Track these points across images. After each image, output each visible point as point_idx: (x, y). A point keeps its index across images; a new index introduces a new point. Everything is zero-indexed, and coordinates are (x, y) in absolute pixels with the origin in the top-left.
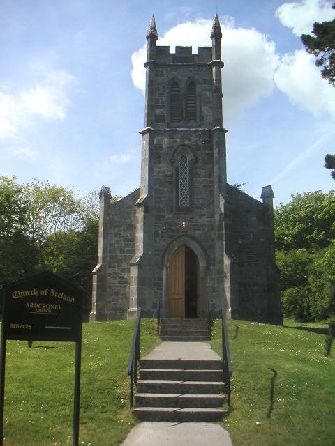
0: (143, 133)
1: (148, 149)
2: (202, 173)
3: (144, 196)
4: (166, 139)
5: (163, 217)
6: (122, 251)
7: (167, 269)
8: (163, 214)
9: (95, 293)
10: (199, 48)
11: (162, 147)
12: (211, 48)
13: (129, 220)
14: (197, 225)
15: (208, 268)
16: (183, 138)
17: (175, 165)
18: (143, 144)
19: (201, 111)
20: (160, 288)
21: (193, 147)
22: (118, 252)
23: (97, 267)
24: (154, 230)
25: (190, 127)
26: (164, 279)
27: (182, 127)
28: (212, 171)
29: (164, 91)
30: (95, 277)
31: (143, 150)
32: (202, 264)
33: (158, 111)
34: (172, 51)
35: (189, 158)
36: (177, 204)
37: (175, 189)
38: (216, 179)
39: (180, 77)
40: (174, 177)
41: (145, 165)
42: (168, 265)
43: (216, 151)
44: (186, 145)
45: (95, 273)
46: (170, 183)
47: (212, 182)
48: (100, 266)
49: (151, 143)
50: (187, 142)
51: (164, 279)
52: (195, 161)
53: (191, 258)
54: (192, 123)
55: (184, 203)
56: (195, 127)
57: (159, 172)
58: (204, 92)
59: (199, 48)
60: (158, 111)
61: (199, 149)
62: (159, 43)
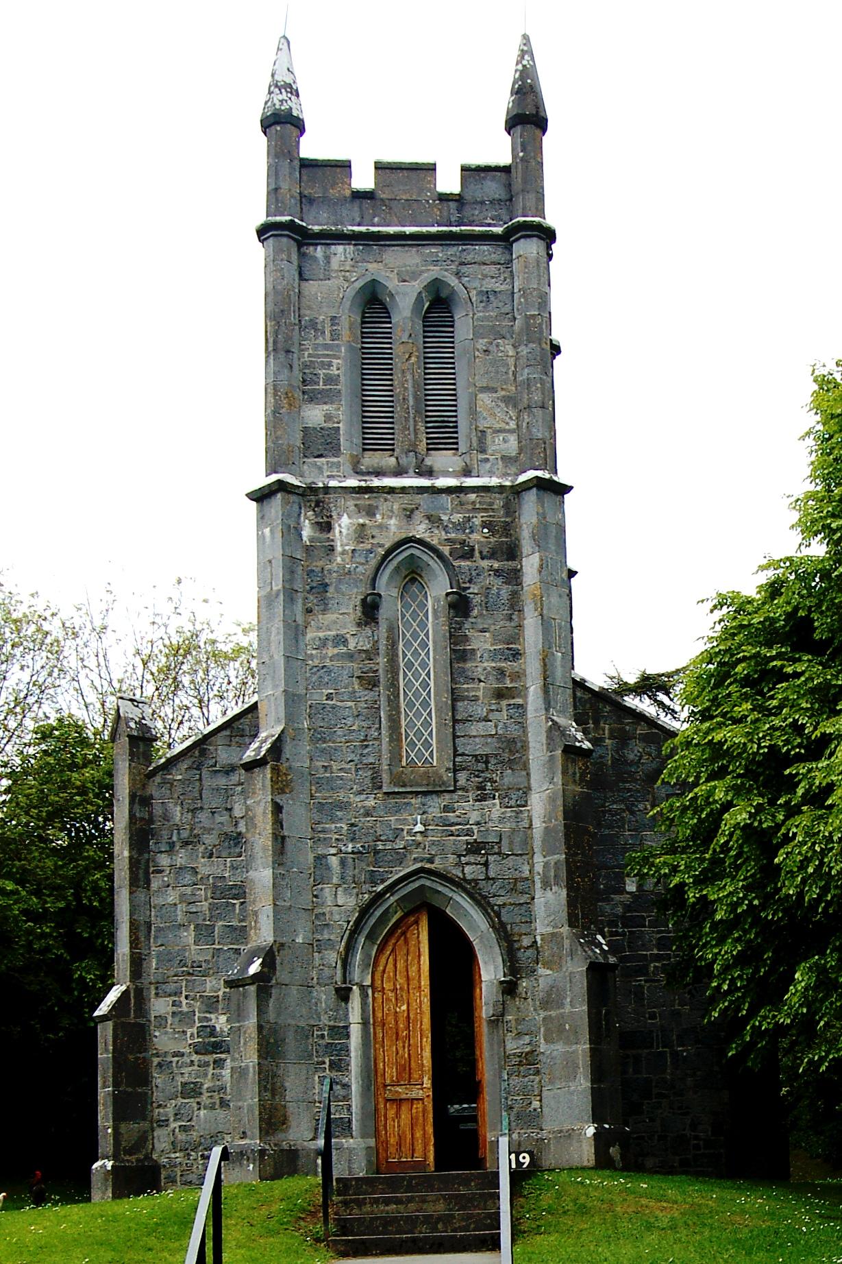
0: (261, 497)
1: (279, 554)
2: (482, 643)
3: (269, 731)
4: (345, 520)
5: (344, 806)
6: (205, 933)
7: (364, 996)
8: (342, 795)
9: (104, 1092)
10: (465, 169)
11: (332, 549)
12: (506, 170)
13: (225, 818)
14: (469, 833)
15: (509, 989)
16: (409, 514)
17: (384, 613)
18: (261, 538)
19: (473, 412)
20: (339, 1065)
21: (446, 550)
22: (189, 936)
23: (113, 996)
24: (311, 857)
25: (429, 473)
26: (355, 1031)
27: (399, 472)
28: (515, 636)
29: (335, 336)
30: (106, 1033)
31: (264, 565)
32: (490, 971)
33: (315, 415)
34: (363, 179)
35: (439, 587)
36: (396, 756)
37: (383, 702)
38: (532, 667)
39: (392, 283)
40: (382, 660)
41: (270, 619)
42: (368, 982)
43: (530, 565)
44: (421, 542)
45: (104, 1018)
46: (370, 682)
47: (517, 676)
48: (125, 994)
49: (291, 532)
50: (420, 530)
51: (355, 1031)
52: (460, 606)
53: (453, 960)
54: (439, 459)
55: (419, 754)
56: (455, 475)
57: (324, 642)
58: (482, 343)
59: (465, 169)
60: (315, 415)
61: (469, 554)
62: (310, 148)
